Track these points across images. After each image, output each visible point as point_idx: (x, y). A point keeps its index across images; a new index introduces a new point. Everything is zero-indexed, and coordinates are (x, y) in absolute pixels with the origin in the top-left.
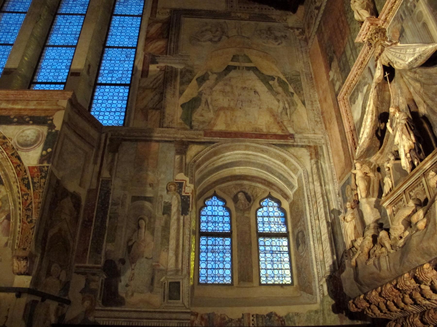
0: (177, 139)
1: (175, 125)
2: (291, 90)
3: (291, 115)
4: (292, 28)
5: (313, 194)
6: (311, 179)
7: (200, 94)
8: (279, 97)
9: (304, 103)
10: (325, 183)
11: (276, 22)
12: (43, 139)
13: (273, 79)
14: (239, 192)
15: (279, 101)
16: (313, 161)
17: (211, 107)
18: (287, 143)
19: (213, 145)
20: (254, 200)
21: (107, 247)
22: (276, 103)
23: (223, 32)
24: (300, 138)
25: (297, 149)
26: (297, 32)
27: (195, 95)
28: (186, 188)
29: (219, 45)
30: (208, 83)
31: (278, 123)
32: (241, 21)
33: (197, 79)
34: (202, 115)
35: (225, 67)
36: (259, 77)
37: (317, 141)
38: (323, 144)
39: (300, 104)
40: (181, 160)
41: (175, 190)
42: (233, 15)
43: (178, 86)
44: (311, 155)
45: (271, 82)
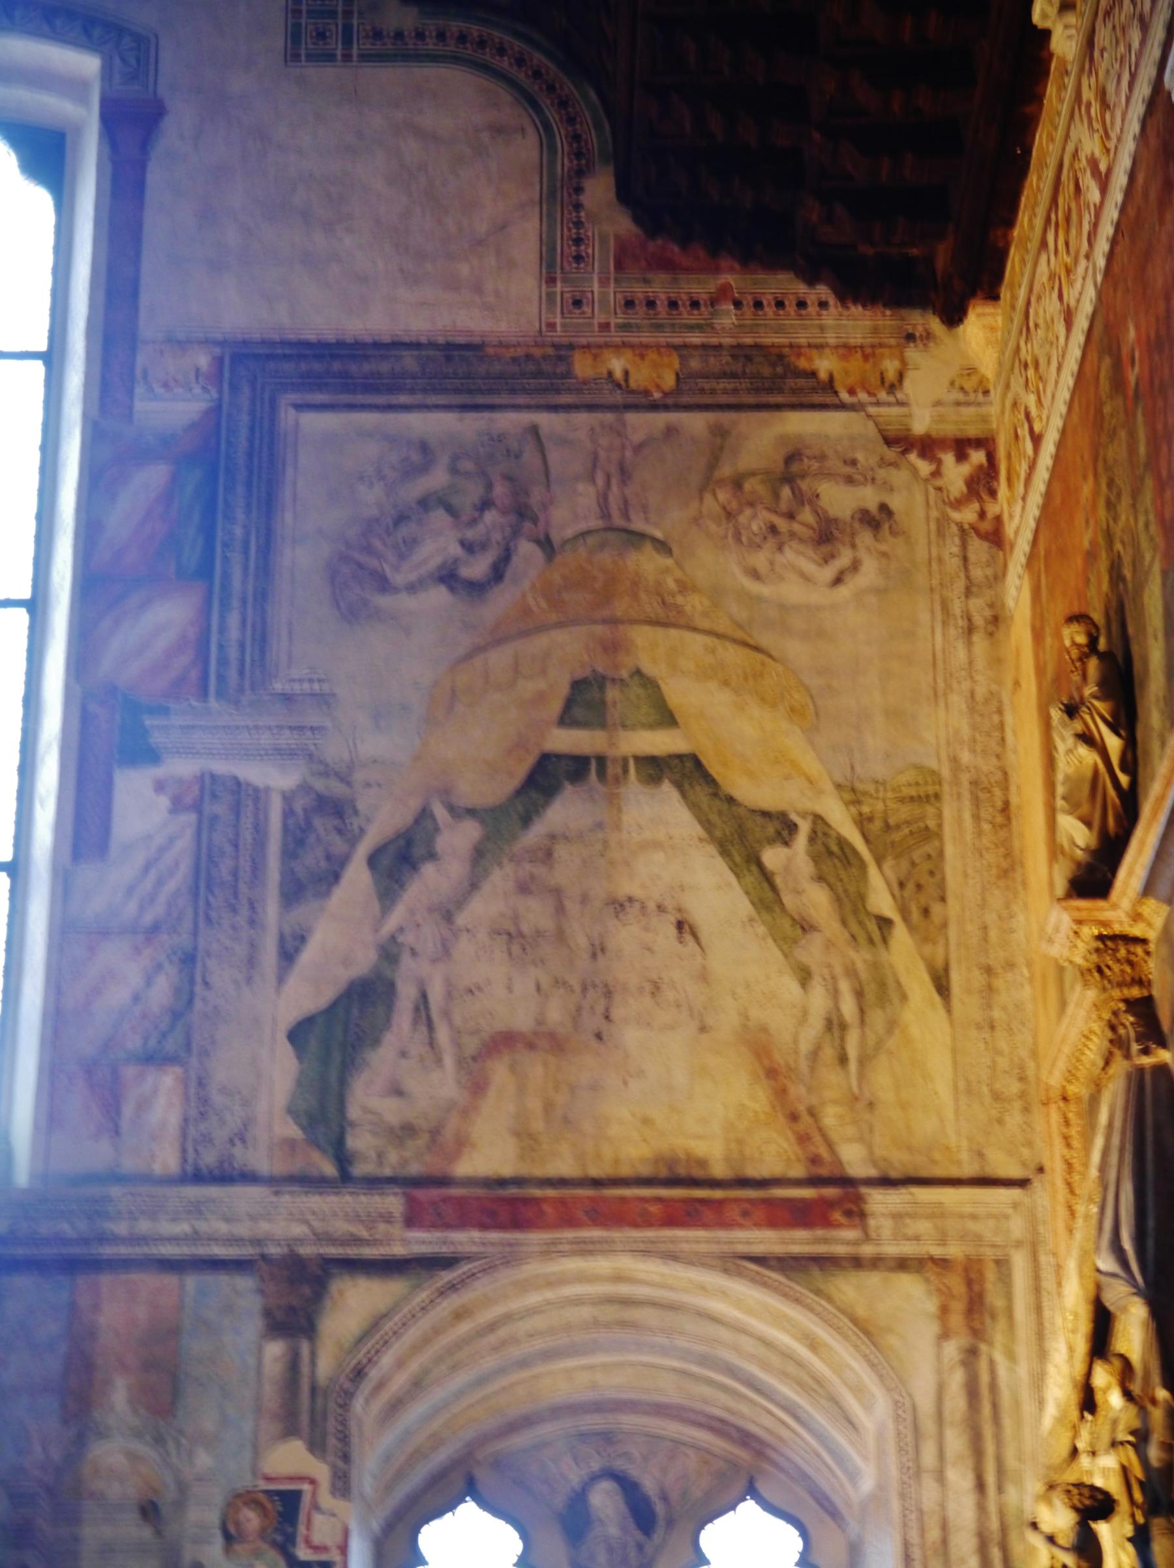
0: (273, 1250)
1: (261, 1161)
2: (882, 901)
3: (864, 1061)
4: (928, 446)
5: (934, 1534)
6: (929, 1457)
7: (390, 953)
8: (812, 952)
9: (942, 986)
10: (1001, 1471)
11: (842, 407)
13: (785, 829)
14: (594, 1478)
15: (804, 976)
16: (952, 1350)
17: (443, 1035)
18: (821, 1249)
19: (447, 1276)
20: (670, 1523)
22: (790, 986)
23: (522, 512)
24: (897, 1217)
25: (873, 1279)
26: (955, 474)
27: (364, 961)
28: (318, 1519)
29: (501, 601)
31: (794, 1117)
32: (632, 417)
33: (373, 861)
34: (397, 1091)
35: (522, 770)
36: (707, 825)
37: (985, 1229)
38: (1018, 1244)
39: (919, 987)
40: (293, 1365)
41: (262, 1534)
42: (582, 367)
43: (271, 909)
44: (944, 1310)
45: (772, 857)
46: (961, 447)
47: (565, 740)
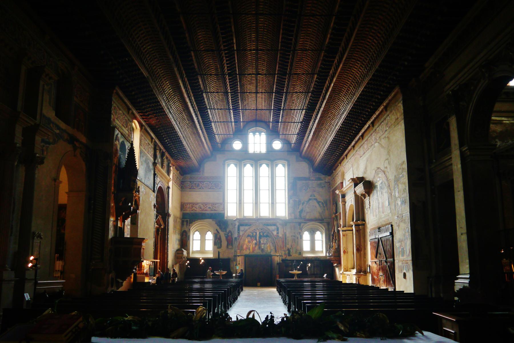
4: (327, 183)
12: (276, 229)
13: (320, 202)
21: (287, 246)
26: (328, 184)
45: (320, 203)
47: (310, 198)
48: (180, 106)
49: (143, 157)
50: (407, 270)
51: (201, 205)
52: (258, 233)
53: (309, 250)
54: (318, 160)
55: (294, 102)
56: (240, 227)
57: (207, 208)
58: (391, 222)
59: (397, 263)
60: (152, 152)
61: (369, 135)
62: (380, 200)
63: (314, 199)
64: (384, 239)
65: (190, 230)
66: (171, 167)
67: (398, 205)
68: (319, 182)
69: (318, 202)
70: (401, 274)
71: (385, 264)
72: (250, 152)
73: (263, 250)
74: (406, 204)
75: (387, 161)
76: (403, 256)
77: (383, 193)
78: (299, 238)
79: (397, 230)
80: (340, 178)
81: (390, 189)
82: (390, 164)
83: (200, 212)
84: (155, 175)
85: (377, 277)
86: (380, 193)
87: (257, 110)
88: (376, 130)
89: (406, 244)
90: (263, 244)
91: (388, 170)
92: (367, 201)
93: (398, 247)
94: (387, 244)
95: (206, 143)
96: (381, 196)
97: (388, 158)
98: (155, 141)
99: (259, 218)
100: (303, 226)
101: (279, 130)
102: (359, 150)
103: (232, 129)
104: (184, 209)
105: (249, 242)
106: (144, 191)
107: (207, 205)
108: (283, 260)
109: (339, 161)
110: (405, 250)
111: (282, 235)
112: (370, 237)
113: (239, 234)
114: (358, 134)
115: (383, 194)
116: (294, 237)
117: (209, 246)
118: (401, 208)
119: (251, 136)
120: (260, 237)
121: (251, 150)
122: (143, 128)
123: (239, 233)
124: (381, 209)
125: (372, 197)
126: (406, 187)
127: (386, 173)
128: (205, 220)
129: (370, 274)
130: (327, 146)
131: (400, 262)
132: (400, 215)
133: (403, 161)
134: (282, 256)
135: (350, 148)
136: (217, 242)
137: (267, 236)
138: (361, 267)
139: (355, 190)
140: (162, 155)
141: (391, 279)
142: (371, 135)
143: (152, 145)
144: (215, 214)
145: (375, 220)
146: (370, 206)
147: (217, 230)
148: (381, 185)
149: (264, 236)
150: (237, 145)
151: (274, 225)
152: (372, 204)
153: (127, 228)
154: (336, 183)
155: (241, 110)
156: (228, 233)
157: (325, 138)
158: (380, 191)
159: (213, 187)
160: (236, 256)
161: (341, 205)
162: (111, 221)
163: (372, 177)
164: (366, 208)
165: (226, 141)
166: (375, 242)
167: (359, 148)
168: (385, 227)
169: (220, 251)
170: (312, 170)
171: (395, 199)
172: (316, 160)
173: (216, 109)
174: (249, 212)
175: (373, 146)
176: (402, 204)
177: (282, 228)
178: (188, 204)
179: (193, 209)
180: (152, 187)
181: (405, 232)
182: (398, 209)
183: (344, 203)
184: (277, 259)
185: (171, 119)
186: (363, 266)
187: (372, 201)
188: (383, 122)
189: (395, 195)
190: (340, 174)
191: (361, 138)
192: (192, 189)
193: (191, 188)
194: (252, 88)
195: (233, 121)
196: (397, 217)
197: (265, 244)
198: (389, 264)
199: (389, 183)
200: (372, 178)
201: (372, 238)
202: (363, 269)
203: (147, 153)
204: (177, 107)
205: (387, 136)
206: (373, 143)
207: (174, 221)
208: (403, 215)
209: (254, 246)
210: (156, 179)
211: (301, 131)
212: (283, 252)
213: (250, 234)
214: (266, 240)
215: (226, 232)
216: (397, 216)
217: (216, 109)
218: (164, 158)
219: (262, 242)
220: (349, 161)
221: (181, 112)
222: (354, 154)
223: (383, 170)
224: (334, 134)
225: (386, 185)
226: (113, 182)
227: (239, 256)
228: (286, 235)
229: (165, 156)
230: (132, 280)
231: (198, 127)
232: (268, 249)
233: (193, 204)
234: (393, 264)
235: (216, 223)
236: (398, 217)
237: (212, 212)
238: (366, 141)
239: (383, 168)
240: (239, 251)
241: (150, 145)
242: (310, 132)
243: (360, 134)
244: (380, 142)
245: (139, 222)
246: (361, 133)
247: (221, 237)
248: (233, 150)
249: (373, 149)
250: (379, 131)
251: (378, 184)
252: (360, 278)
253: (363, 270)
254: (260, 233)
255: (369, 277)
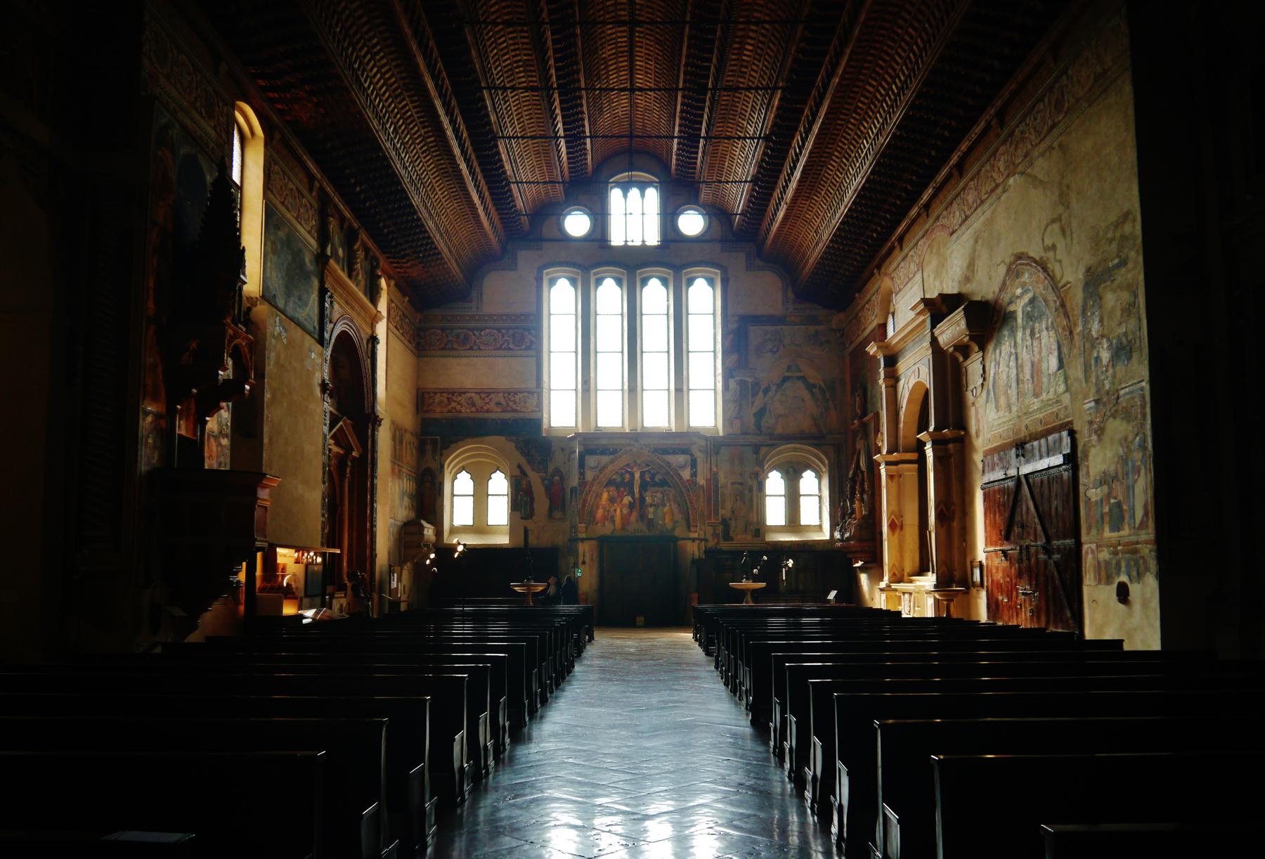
7: (765, 404)
12: (689, 462)
13: (814, 386)
21: (721, 512)
30: (771, 393)
43: (750, 398)
46: (840, 330)
47: (788, 374)
48: (392, 68)
49: (277, 228)
50: (1134, 573)
51: (473, 395)
52: (637, 475)
53: (784, 524)
54: (807, 269)
55: (746, 73)
56: (587, 457)
57: (492, 403)
58: (1071, 422)
59: (1093, 552)
60: (314, 222)
61: (984, 158)
62: (1025, 356)
63: (799, 378)
64: (1038, 479)
65: (442, 466)
66: (380, 277)
67: (1101, 360)
68: (812, 329)
69: (810, 387)
70: (1108, 588)
71: (1042, 557)
72: (613, 244)
73: (650, 523)
74: (1135, 355)
75: (1056, 226)
76: (1116, 527)
77: (1037, 330)
78: (755, 489)
79: (1094, 446)
80: (877, 311)
81: (1066, 315)
82: (1068, 233)
83: (472, 415)
84: (323, 292)
85: (1010, 599)
86: (1024, 333)
87: (632, 90)
88: (1011, 134)
89: (1130, 489)
90: (651, 505)
91: (1061, 253)
92: (973, 367)
93: (1096, 502)
94: (1053, 494)
95: (486, 209)
96: (1029, 343)
97: (1060, 215)
98: (321, 188)
99: (639, 431)
100: (767, 454)
101: (698, 171)
102: (945, 213)
103: (561, 167)
104: (425, 408)
105: (612, 500)
106: (284, 334)
107: (492, 396)
108: (707, 552)
109: (876, 261)
110: (1125, 507)
111: (707, 481)
112: (983, 478)
113: (584, 479)
114: (947, 158)
115: (1037, 335)
116: (739, 487)
117: (499, 512)
118: (1111, 371)
119: (615, 194)
120: (644, 486)
121: (616, 239)
122: (277, 136)
123: (582, 474)
124: (1028, 386)
125: (995, 350)
126: (1136, 296)
127: (1049, 265)
128: (487, 438)
129: (980, 589)
130: (843, 210)
131: (1105, 549)
132: (1108, 393)
133: (1125, 210)
134: (706, 540)
135: (914, 212)
136: (520, 501)
137: (664, 483)
138: (951, 570)
139: (937, 332)
140: (350, 238)
141: (1065, 603)
142: (994, 154)
143: (310, 199)
144: (516, 421)
145: (1004, 423)
146: (984, 379)
147: (519, 467)
148: (1029, 309)
149: (655, 484)
150: (577, 224)
151: (685, 451)
152: (992, 372)
153: (219, 444)
154: (865, 328)
155: (584, 93)
156: (553, 476)
157: (838, 185)
158: (1024, 329)
159: (509, 344)
160: (574, 541)
161: (883, 386)
162: (147, 414)
163: (996, 287)
164: (971, 387)
165: (548, 211)
166: (1003, 491)
167: (946, 209)
168: (1043, 441)
169: (530, 527)
170: (790, 294)
171: (1088, 345)
172: (807, 261)
173: (509, 88)
174: (610, 416)
175: (1000, 189)
176: (1115, 357)
177: (707, 462)
178: (436, 393)
179: (450, 407)
180: (314, 327)
181: (1130, 450)
182: (1097, 377)
183: (891, 382)
184: (693, 549)
185: (363, 107)
186: (956, 566)
187: (993, 364)
188: (1041, 99)
189: (1087, 331)
190: (877, 299)
191: (956, 173)
192: (449, 349)
193: (448, 348)
194: (619, 34)
195: (561, 133)
196: (1093, 404)
197: (656, 506)
198: (1056, 556)
199: (1063, 295)
200: (994, 292)
201: (992, 480)
202: (957, 574)
203: (294, 222)
204: (383, 70)
205: (1055, 144)
206: (999, 180)
207: (394, 438)
208: (1122, 392)
209: (625, 511)
210: (327, 305)
211: (765, 169)
212: (710, 530)
213: (614, 477)
214: (659, 495)
215: (546, 472)
216: (1094, 400)
217: (509, 88)
218: (356, 247)
219: (648, 500)
220: (910, 254)
221: (399, 91)
222: (927, 231)
223: (1037, 258)
224: (870, 166)
225: (1052, 304)
226: (151, 284)
227: (582, 542)
228: (717, 481)
229: (360, 241)
230: (242, 608)
231: (457, 151)
232: (667, 521)
233: (453, 393)
234: (1074, 557)
235: (517, 447)
236: (1097, 402)
237: (507, 416)
238: (972, 179)
239: (1035, 251)
240: (583, 525)
241: (303, 197)
242: (793, 169)
243: (954, 159)
244: (1029, 171)
245: (266, 429)
246: (959, 153)
247: (531, 487)
248: (567, 239)
249: (999, 198)
250: (1027, 135)
251: (1019, 307)
252: (953, 600)
253: (956, 579)
254: (642, 474)
255: (978, 597)
